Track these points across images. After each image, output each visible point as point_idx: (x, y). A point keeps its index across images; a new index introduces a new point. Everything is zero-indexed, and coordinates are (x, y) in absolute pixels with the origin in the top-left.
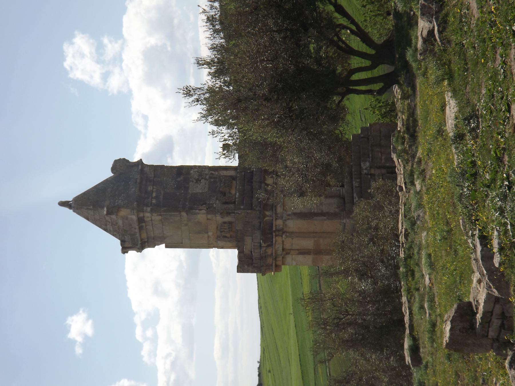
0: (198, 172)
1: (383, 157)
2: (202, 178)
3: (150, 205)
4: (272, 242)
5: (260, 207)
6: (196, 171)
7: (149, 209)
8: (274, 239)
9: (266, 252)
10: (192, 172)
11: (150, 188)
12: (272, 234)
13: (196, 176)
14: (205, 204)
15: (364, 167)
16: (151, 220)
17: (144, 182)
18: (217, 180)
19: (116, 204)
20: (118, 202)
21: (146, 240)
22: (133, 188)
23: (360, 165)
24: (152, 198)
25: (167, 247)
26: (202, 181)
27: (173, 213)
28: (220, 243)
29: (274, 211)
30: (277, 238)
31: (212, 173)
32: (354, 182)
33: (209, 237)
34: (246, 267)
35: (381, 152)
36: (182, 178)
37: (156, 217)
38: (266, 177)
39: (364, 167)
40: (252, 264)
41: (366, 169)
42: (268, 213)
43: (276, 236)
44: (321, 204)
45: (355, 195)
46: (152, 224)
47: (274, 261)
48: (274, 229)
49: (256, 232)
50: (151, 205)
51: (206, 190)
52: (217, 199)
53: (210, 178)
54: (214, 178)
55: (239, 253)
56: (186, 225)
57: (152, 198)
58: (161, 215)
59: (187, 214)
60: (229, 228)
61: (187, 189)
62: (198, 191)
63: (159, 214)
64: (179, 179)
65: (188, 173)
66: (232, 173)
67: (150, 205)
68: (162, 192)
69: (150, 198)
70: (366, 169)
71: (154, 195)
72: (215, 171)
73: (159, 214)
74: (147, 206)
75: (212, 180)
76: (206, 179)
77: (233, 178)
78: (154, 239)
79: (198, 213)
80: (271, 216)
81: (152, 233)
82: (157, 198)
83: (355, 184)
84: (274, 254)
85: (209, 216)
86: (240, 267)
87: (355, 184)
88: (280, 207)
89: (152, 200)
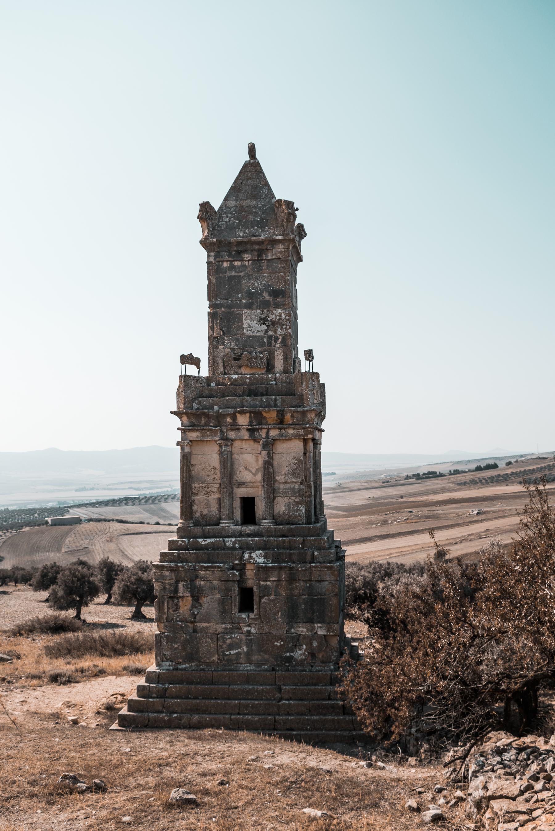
0: (279, 319)
1: (269, 583)
2: (268, 326)
3: (218, 259)
5: (198, 408)
6: (280, 316)
7: (212, 259)
10: (280, 311)
14: (224, 334)
15: (253, 555)
17: (257, 247)
18: (266, 347)
19: (225, 216)
20: (227, 217)
22: (245, 233)
23: (259, 549)
24: (231, 262)
26: (264, 327)
29: (190, 428)
31: (278, 339)
32: (233, 539)
35: (279, 581)
36: (267, 298)
38: (248, 415)
39: (253, 555)
41: (250, 557)
44: (208, 493)
45: (213, 540)
50: (219, 261)
51: (249, 333)
52: (233, 349)
53: (270, 337)
54: (270, 344)
57: (231, 262)
61: (249, 306)
62: (245, 322)
64: (265, 294)
65: (277, 306)
67: (218, 259)
68: (242, 274)
69: (230, 259)
70: (250, 557)
71: (237, 263)
72: (281, 342)
74: (216, 257)
75: (265, 340)
76: (266, 331)
82: (232, 267)
83: (230, 542)
87: (230, 542)
88: (197, 437)
89: (227, 261)
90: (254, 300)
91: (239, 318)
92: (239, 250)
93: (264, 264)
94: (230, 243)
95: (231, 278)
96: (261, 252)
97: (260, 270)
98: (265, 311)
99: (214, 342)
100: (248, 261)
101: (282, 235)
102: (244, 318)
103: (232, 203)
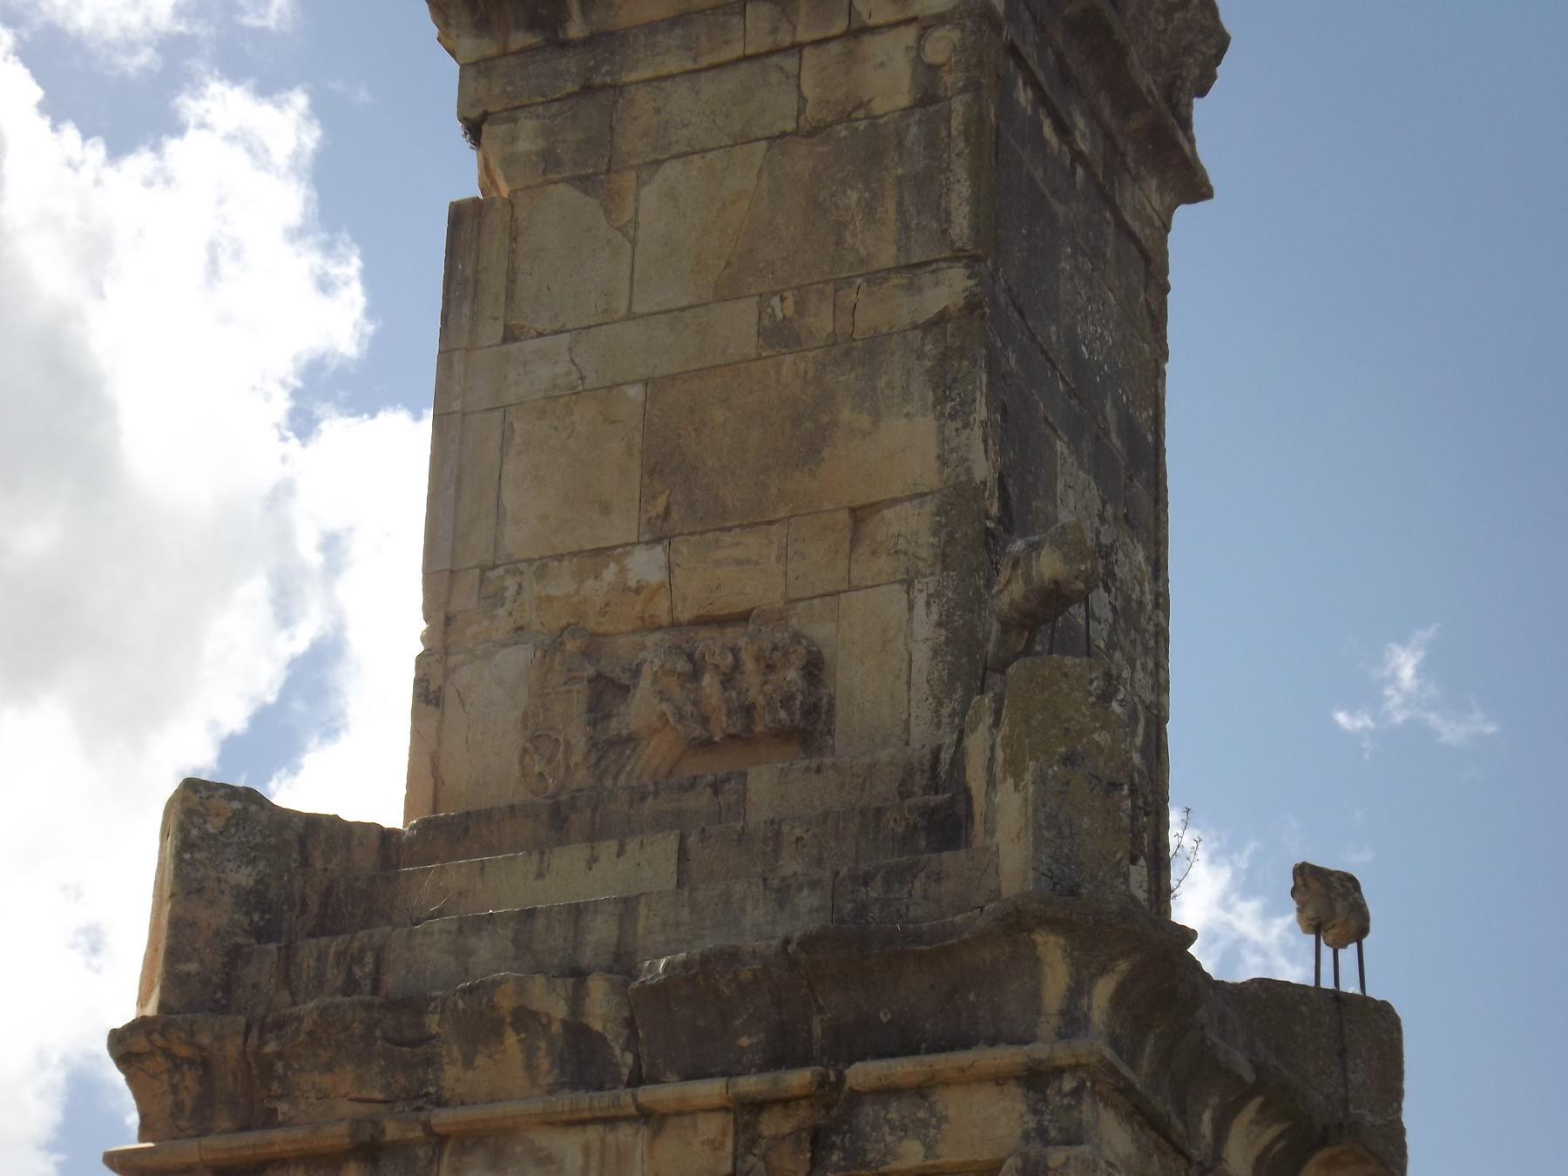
4: (636, 1080)
8: (710, 1090)
9: (482, 1025)
12: (778, 1060)
16: (858, 32)
21: (576, 29)
25: (462, 217)
27: (961, 189)
28: (502, 677)
30: (712, 1126)
33: (601, 554)
34: (243, 877)
37: (887, 77)
40: (261, 934)
42: (1103, 990)
43: (747, 1110)
46: (798, 47)
47: (336, 1134)
48: (863, 1074)
49: (806, 900)
55: (387, 835)
56: (780, 336)
58: (928, 96)
59: (942, 318)
60: (749, 710)
63: (951, 80)
68: (1059, 208)
73: (951, 80)
78: (587, 89)
79: (961, 414)
80: (1073, 1021)
81: (672, 65)
84: (443, 1118)
85: (911, 526)
86: (240, 819)
98: (1110, 509)
100: (1078, 156)
102: (1060, 487)
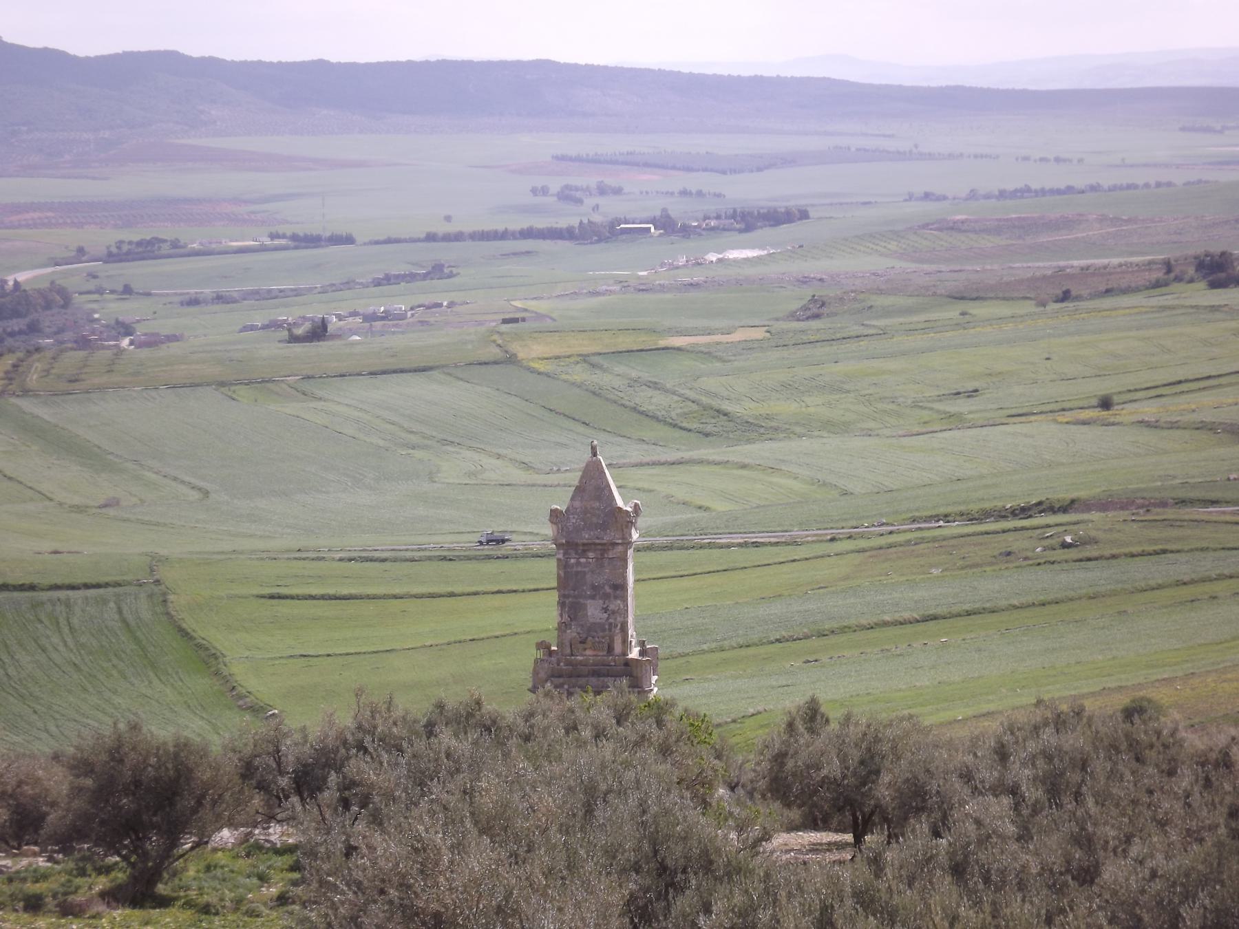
11: (591, 555)
13: (612, 607)
26: (606, 615)
51: (591, 620)
54: (610, 630)
61: (593, 597)
64: (607, 589)
65: (616, 598)
66: (618, 648)
71: (583, 560)
74: (564, 554)
77: (610, 649)
82: (578, 563)
90: (597, 592)
91: (584, 607)
92: (587, 547)
93: (606, 562)
94: (577, 544)
95: (577, 573)
96: (604, 551)
97: (602, 566)
99: (562, 627)
101: (623, 538)
103: (577, 504)
